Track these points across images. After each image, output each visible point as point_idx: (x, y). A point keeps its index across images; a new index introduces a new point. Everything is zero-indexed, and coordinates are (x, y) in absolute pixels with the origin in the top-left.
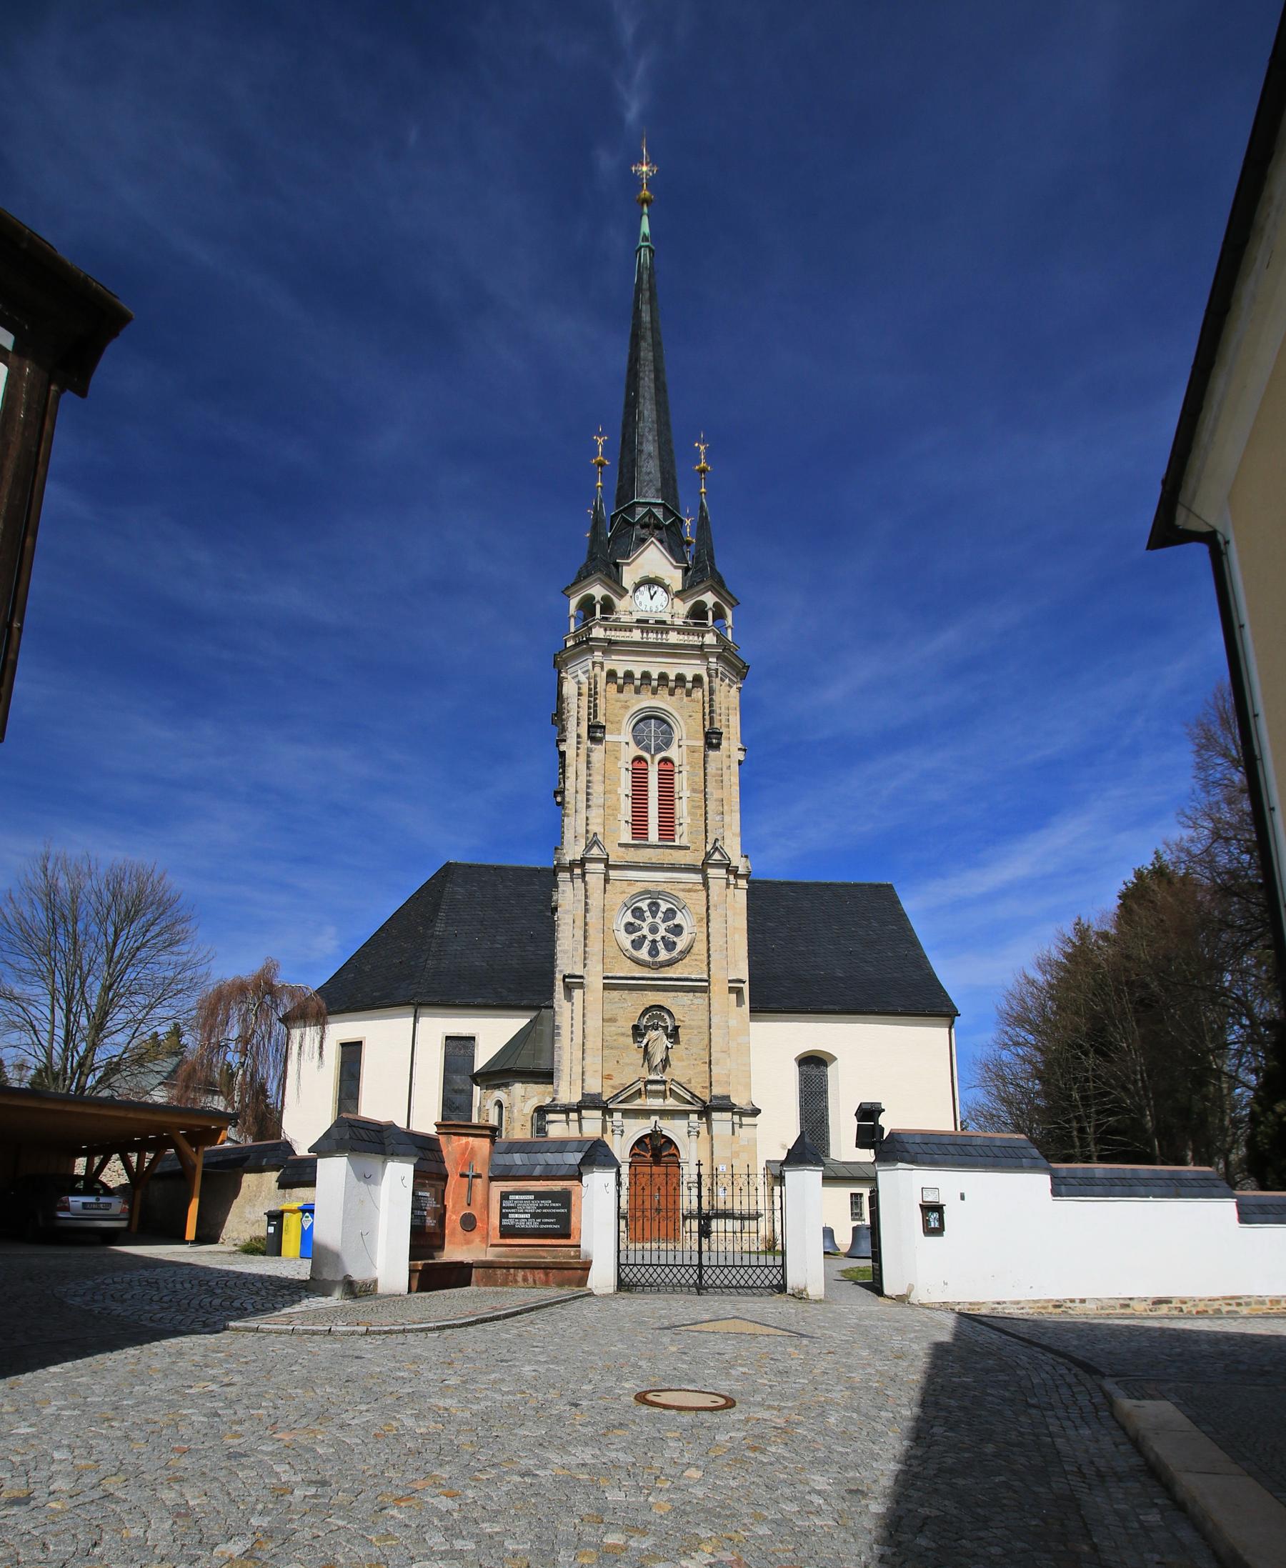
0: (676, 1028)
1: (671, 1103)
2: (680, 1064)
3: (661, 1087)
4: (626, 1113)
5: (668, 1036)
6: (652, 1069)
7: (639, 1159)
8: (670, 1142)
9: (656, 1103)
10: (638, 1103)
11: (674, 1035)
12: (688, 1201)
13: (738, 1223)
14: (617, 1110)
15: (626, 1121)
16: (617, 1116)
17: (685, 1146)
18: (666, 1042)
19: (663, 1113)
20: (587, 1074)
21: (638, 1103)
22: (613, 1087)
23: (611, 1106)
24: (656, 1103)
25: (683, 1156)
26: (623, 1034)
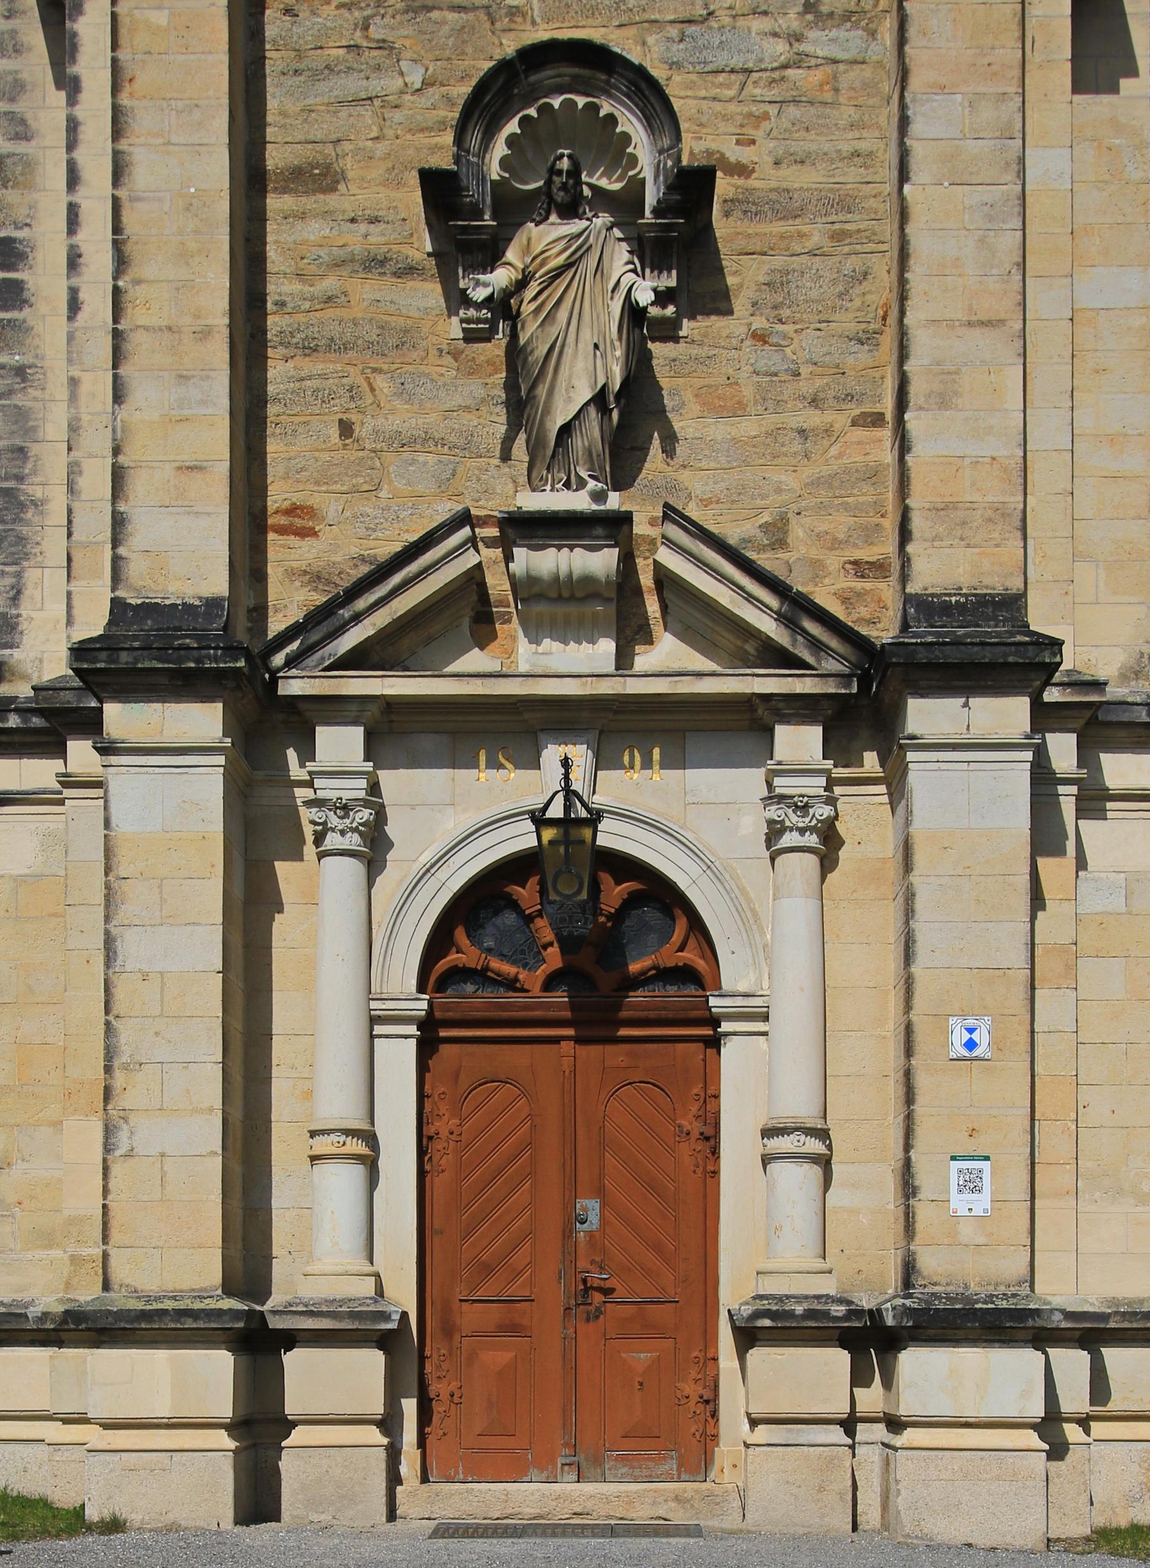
0: (693, 187)
1: (669, 662)
2: (719, 430)
3: (601, 562)
4: (395, 732)
5: (651, 252)
6: (551, 456)
7: (471, 998)
8: (659, 895)
9: (578, 663)
10: (468, 673)
11: (681, 231)
12: (770, 1232)
13: (1071, 1364)
14: (334, 709)
15: (392, 781)
16: (340, 744)
17: (749, 919)
18: (626, 278)
19: (622, 726)
20: (139, 486)
21: (468, 673)
22: (315, 578)
23: (294, 686)
24: (578, 663)
25: (737, 971)
26: (375, 263)
